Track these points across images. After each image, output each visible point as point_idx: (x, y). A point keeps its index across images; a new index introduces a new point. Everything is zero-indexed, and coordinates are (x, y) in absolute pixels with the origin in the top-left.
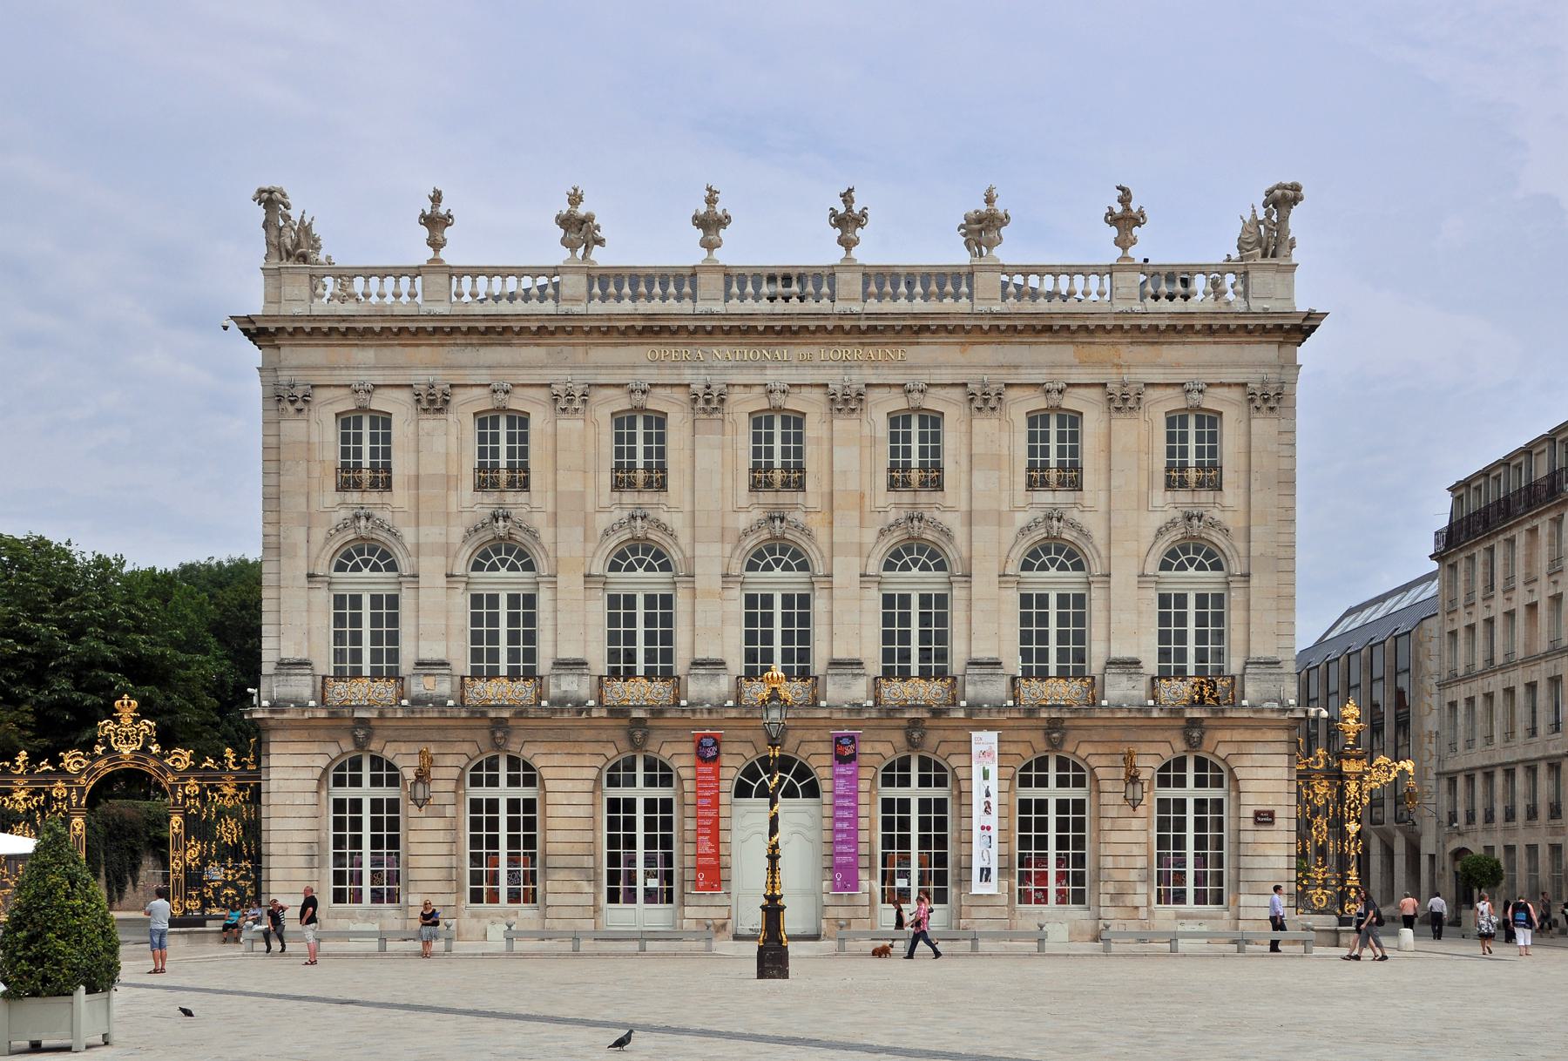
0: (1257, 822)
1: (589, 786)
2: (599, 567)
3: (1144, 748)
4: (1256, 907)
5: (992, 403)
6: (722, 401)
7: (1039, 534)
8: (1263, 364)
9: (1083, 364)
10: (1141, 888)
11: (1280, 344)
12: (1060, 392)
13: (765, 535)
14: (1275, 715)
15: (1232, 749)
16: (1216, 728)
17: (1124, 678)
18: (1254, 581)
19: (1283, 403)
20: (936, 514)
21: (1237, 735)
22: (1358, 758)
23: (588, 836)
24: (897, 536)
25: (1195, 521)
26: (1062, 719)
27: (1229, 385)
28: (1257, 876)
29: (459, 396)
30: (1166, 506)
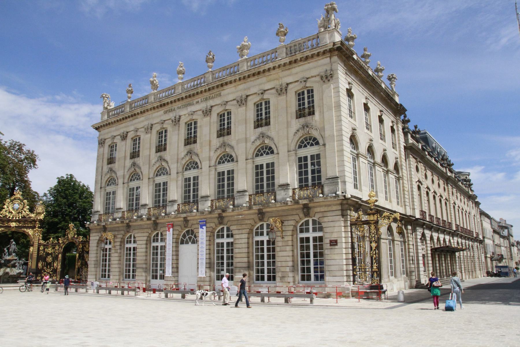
0: (331, 245)
1: (145, 242)
2: (151, 175)
3: (290, 218)
4: (331, 281)
5: (243, 102)
6: (179, 121)
7: (258, 143)
8: (325, 65)
9: (269, 81)
10: (291, 275)
11: (330, 57)
12: (262, 93)
13: (187, 159)
14: (332, 199)
15: (320, 215)
16: (314, 207)
17: (282, 191)
18: (327, 146)
19: (334, 78)
20: (230, 143)
21: (322, 209)
22: (373, 214)
23: (144, 258)
24: (219, 152)
25: (305, 127)
26: (262, 209)
27: (315, 76)
28: (332, 268)
29: (129, 134)
30: (296, 124)
